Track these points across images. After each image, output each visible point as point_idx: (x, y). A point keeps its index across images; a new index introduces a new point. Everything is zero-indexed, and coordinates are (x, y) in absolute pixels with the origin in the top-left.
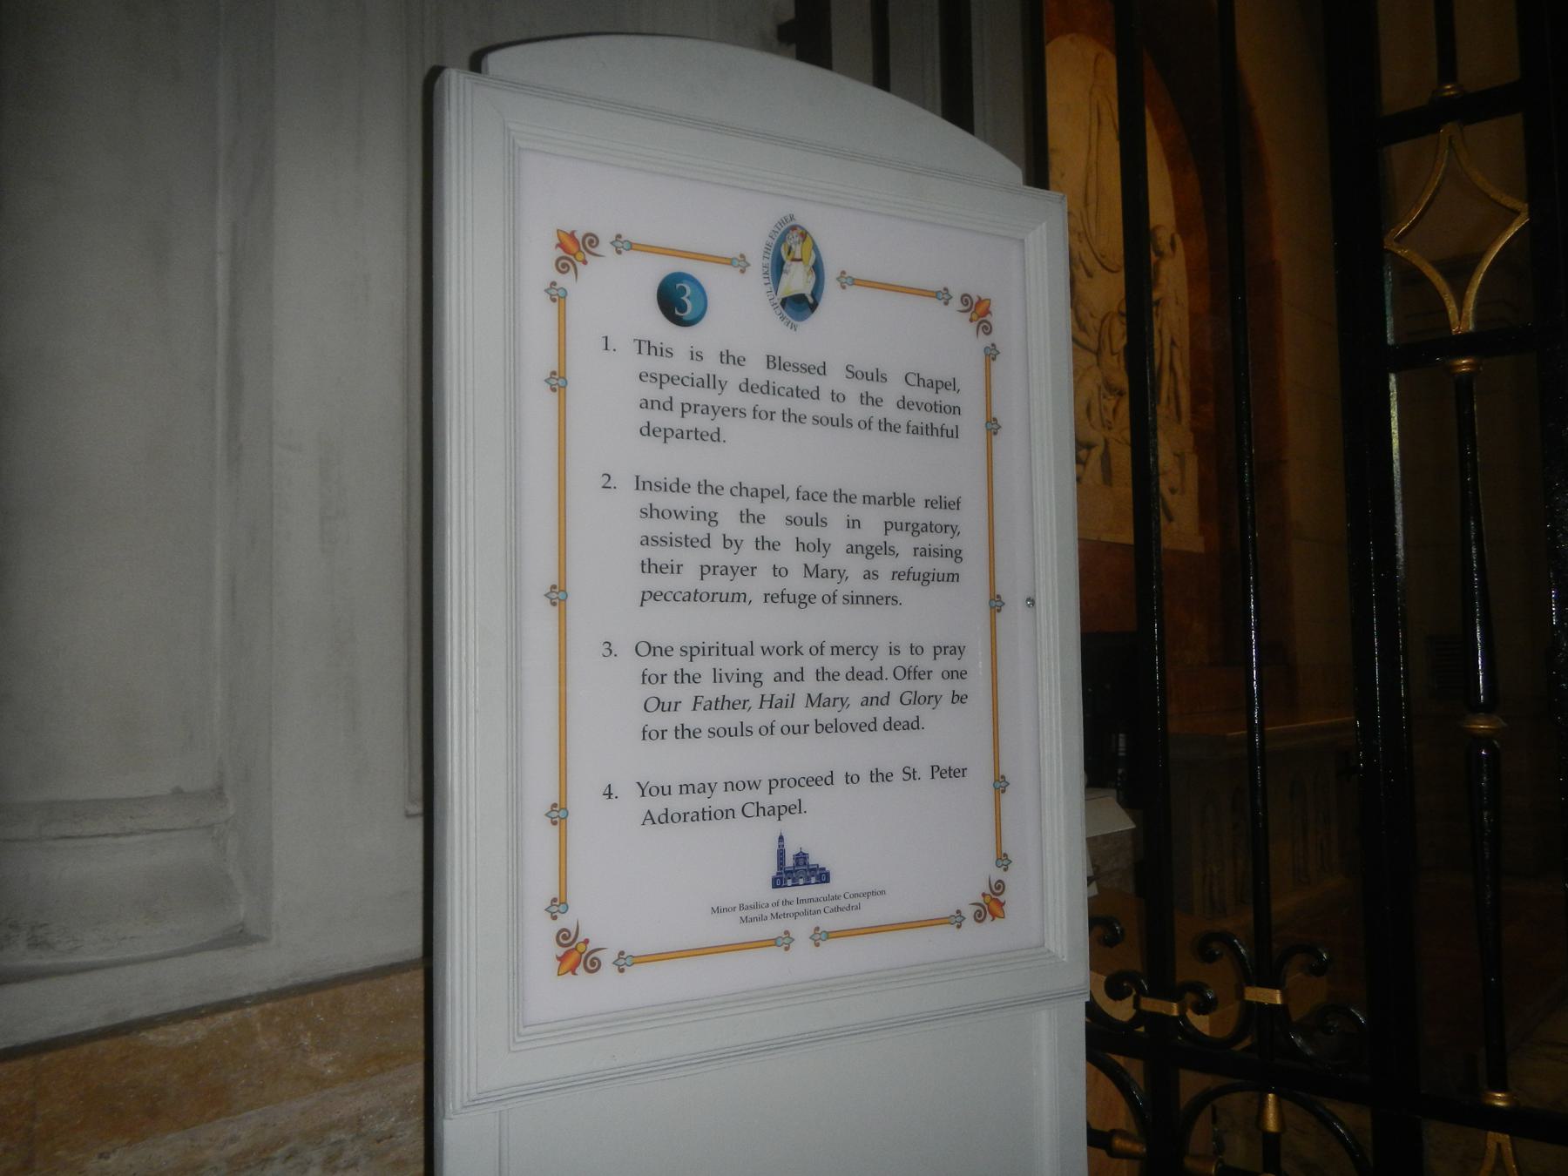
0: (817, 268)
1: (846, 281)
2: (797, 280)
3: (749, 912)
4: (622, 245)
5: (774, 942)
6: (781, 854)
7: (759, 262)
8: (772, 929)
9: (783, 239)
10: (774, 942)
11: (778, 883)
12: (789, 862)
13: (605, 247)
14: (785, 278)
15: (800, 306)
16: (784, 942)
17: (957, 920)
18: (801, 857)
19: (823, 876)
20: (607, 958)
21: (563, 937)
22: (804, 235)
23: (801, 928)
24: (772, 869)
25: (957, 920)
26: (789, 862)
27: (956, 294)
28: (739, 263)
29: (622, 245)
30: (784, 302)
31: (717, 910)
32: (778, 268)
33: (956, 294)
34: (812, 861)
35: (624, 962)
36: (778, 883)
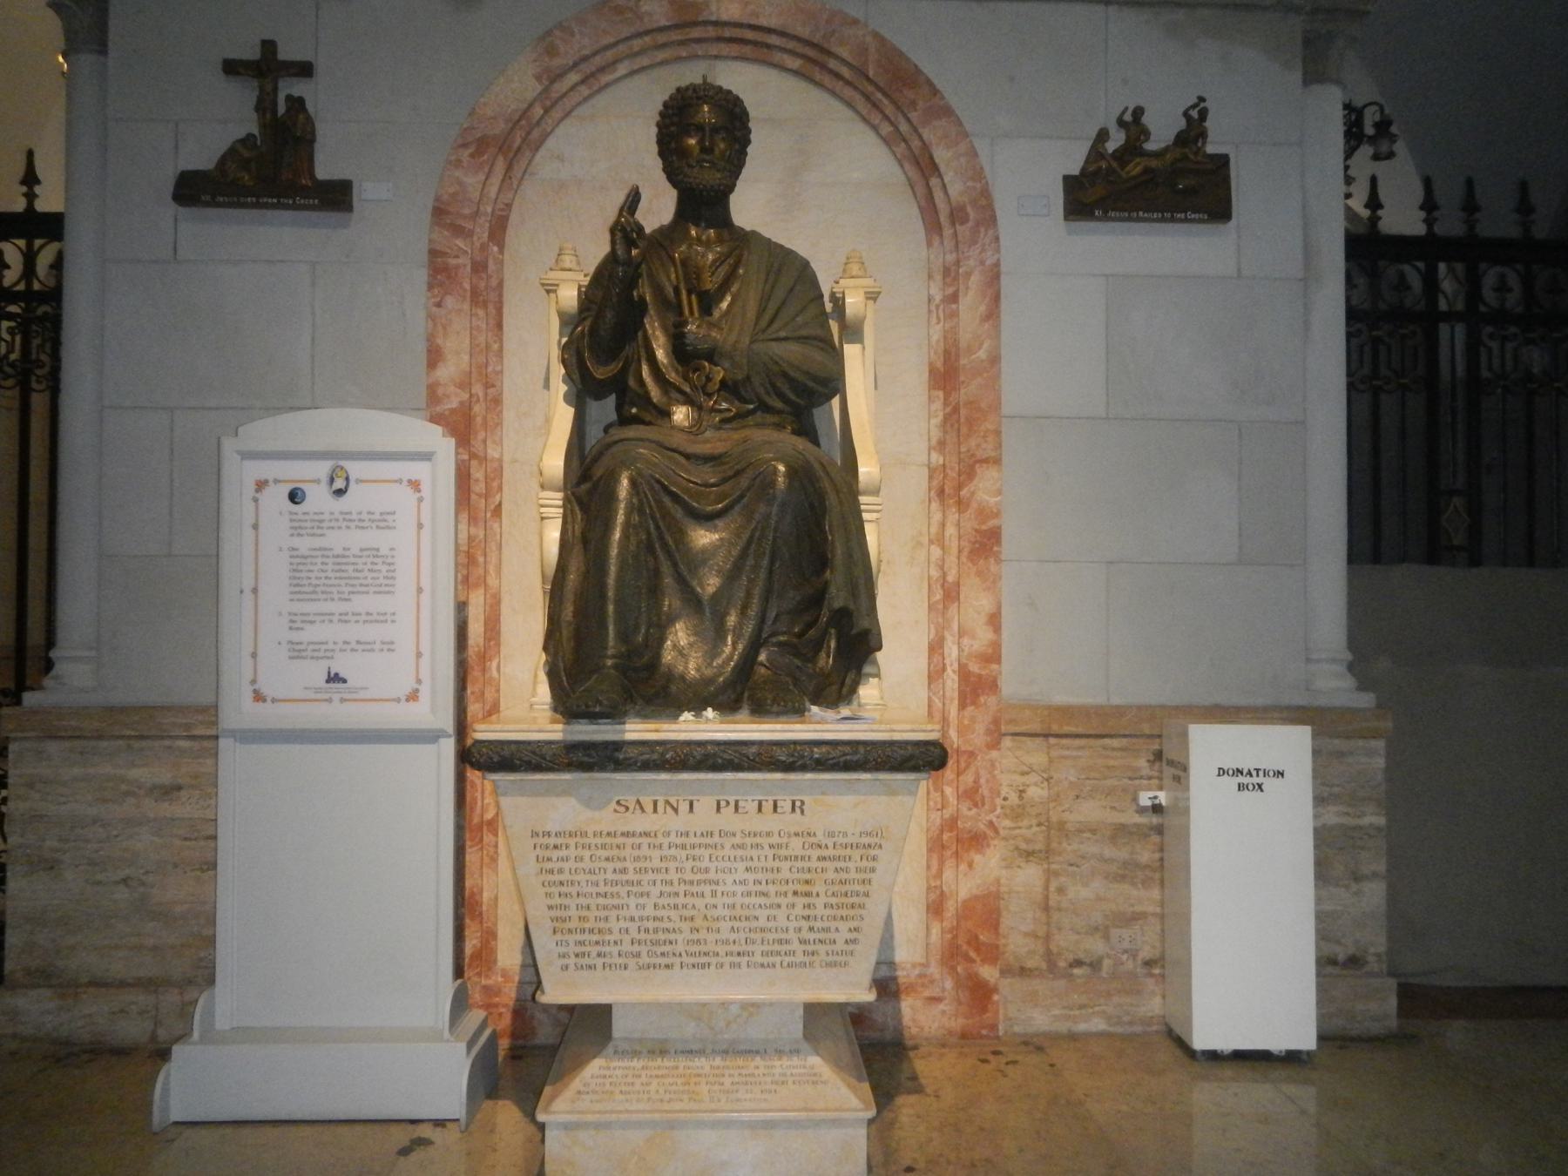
0: (347, 479)
1: (358, 481)
2: (339, 484)
3: (318, 690)
4: (277, 481)
5: (326, 700)
6: (329, 673)
7: (325, 479)
8: (326, 696)
9: (334, 471)
10: (326, 700)
11: (328, 681)
12: (332, 675)
13: (271, 483)
14: (334, 484)
15: (340, 493)
16: (330, 700)
17: (398, 700)
18: (336, 674)
19: (345, 681)
20: (269, 699)
21: (255, 691)
22: (342, 468)
23: (336, 697)
24: (326, 677)
25: (398, 700)
26: (332, 675)
27: (405, 480)
28: (318, 481)
29: (277, 481)
30: (334, 492)
31: (306, 688)
32: (332, 480)
33: (405, 480)
34: (341, 675)
35: (274, 700)
36: (328, 681)
